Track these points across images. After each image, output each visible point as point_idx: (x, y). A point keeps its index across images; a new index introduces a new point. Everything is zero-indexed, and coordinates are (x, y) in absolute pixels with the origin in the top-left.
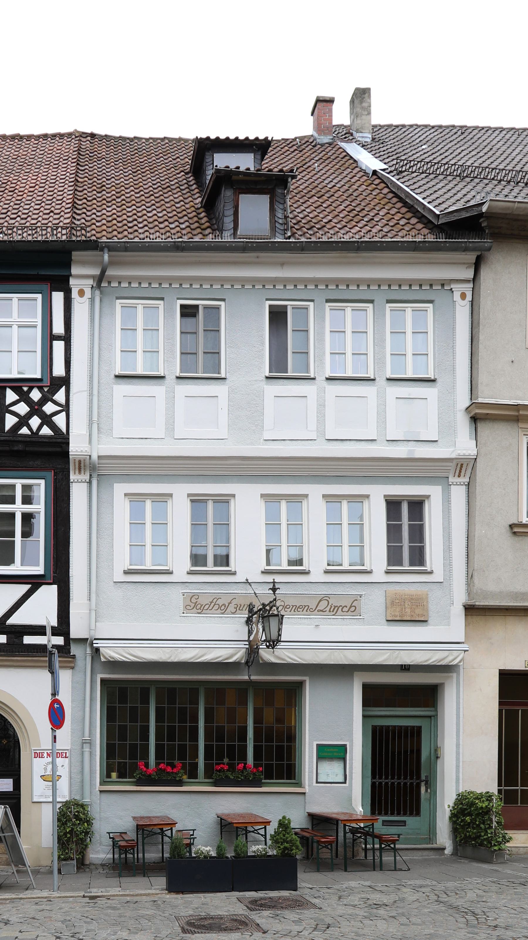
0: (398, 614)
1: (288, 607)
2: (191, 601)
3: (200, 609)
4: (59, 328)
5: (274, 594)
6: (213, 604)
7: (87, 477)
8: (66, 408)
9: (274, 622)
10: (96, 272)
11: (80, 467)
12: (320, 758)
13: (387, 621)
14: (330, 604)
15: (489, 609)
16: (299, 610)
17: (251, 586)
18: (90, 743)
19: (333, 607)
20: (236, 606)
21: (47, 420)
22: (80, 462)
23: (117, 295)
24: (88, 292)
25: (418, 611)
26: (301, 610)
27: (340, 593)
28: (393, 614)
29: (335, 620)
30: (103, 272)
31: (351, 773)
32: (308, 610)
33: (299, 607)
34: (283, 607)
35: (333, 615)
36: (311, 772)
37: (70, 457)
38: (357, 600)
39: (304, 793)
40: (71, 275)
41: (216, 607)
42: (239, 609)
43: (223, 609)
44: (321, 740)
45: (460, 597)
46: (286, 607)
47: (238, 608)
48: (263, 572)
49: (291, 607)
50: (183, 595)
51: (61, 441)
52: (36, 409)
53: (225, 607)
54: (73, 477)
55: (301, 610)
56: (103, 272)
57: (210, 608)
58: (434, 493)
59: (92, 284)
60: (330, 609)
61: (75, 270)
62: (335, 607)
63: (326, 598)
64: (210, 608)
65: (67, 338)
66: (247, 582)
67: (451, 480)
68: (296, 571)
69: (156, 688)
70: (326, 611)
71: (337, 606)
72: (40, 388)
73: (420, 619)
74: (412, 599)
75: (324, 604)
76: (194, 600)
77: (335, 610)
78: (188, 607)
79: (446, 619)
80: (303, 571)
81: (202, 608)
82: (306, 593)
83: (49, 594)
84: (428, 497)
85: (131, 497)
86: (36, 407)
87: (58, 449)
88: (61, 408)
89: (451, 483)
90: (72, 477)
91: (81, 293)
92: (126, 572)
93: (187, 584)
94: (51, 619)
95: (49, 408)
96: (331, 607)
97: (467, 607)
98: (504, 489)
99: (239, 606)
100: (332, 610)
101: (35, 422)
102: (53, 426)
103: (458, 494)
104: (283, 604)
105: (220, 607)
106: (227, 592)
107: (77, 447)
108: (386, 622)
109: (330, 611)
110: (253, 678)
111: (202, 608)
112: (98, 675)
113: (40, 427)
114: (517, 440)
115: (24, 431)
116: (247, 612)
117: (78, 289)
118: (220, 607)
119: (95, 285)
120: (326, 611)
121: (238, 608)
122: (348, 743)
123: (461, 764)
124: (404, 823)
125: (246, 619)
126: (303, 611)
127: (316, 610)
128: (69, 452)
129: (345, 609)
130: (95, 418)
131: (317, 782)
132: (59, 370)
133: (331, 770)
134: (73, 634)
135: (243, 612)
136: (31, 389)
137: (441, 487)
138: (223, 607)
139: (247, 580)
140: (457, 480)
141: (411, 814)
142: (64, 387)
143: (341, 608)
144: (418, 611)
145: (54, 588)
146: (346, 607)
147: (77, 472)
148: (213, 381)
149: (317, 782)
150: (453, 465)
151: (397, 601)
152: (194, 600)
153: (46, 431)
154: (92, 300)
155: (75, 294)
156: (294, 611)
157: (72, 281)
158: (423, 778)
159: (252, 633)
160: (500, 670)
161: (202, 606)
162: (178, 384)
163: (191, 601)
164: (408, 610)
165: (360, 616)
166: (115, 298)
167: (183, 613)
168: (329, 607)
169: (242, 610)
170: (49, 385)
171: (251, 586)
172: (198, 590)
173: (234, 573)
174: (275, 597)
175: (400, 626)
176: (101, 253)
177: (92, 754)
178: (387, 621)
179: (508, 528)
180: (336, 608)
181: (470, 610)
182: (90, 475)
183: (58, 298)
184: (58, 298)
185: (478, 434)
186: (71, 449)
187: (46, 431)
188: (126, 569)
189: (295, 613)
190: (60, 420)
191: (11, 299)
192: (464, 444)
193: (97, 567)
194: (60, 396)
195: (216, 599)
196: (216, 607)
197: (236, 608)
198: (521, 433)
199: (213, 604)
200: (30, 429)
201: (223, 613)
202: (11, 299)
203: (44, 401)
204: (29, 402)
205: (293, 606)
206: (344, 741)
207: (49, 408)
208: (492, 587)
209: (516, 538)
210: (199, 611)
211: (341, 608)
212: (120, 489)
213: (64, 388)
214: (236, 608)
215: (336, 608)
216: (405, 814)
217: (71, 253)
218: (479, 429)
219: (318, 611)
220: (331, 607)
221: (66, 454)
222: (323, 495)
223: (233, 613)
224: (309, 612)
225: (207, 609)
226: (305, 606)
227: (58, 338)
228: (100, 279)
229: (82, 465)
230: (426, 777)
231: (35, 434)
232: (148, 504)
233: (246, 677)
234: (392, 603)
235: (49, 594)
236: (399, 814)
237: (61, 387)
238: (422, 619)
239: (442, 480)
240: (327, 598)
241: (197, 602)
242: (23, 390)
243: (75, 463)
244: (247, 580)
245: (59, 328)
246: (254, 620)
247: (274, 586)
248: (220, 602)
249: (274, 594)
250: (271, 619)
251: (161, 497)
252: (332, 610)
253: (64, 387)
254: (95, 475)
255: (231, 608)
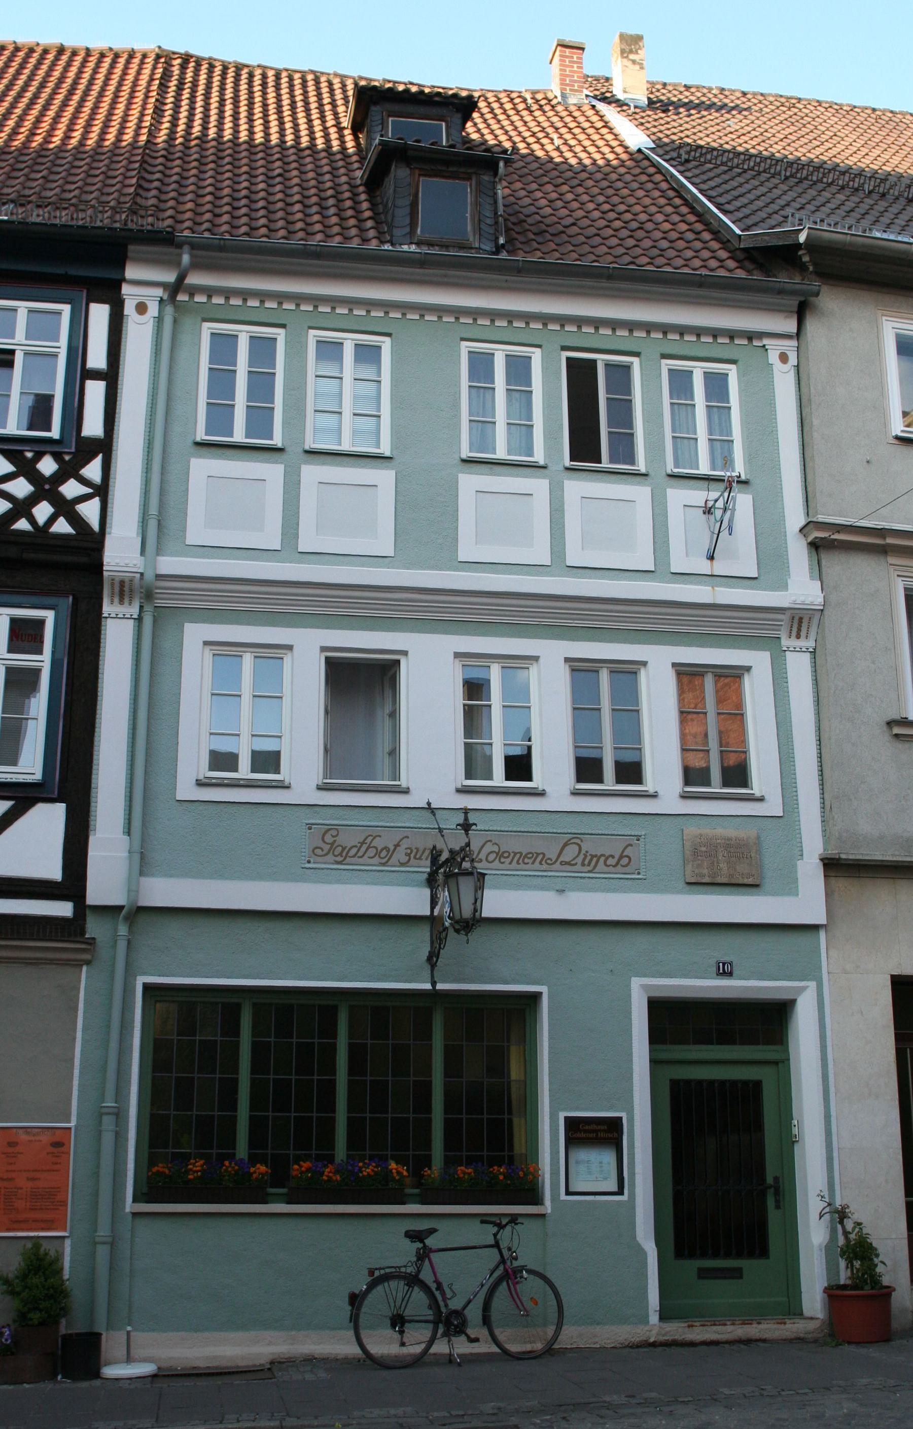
0: (706, 871)
1: (506, 855)
2: (323, 839)
3: (341, 854)
4: (97, 358)
5: (467, 834)
6: (365, 847)
7: (134, 610)
8: (102, 491)
9: (466, 886)
10: (170, 277)
11: (124, 590)
12: (571, 1142)
13: (689, 884)
14: (583, 852)
15: (865, 866)
16: (526, 860)
17: (434, 815)
18: (119, 1115)
19: (589, 858)
20: (409, 851)
21: (65, 508)
22: (122, 583)
23: (205, 316)
24: (153, 309)
25: (742, 868)
26: (530, 861)
27: (600, 832)
28: (696, 871)
29: (593, 881)
30: (181, 278)
31: (632, 1174)
32: (543, 862)
33: (526, 856)
34: (497, 854)
35: (589, 872)
36: (555, 1173)
37: (105, 573)
38: (631, 845)
39: (543, 1216)
40: (124, 280)
41: (372, 852)
42: (415, 858)
43: (385, 855)
44: (571, 1110)
45: (813, 846)
46: (502, 856)
47: (412, 856)
48: (458, 791)
49: (512, 854)
50: (310, 829)
51: (89, 544)
52: (46, 489)
53: (388, 851)
54: (107, 608)
55: (530, 861)
56: (181, 278)
57: (360, 854)
58: (758, 661)
59: (161, 295)
60: (584, 860)
61: (132, 272)
62: (593, 856)
63: (574, 839)
64: (360, 854)
65: (111, 376)
66: (430, 808)
67: (785, 642)
68: (513, 790)
69: (254, 1005)
70: (576, 864)
71: (596, 856)
72: (57, 457)
73: (746, 881)
74: (729, 846)
75: (570, 853)
76: (329, 838)
77: (592, 861)
78: (318, 851)
79: (789, 886)
80: (533, 791)
81: (344, 854)
82: (539, 830)
83: (48, 821)
84: (748, 669)
85: (214, 648)
86: (47, 487)
87: (84, 560)
88: (91, 491)
89: (785, 649)
90: (107, 609)
91: (141, 308)
92: (200, 784)
93: (317, 809)
94: (52, 869)
95: (71, 489)
96: (586, 856)
97: (826, 861)
98: (873, 663)
99: (415, 851)
100: (586, 862)
101: (43, 511)
102: (76, 520)
103: (799, 667)
104: (496, 849)
105: (378, 853)
106: (392, 824)
107: (121, 554)
108: (685, 885)
109: (583, 865)
110: (439, 986)
111: (344, 854)
112: (138, 978)
113: (52, 520)
114: (892, 583)
115: (22, 525)
116: (428, 863)
117: (136, 302)
118: (378, 853)
119: (165, 297)
120: (576, 864)
121: (413, 854)
122: (624, 1115)
123: (835, 1154)
124: (736, 1274)
125: (425, 876)
126: (533, 863)
127: (558, 862)
128: (102, 565)
129: (611, 861)
130: (153, 510)
131: (568, 1193)
132: (93, 426)
133: (594, 1168)
134: (92, 898)
135: (423, 863)
136: (39, 456)
137: (767, 654)
138: (384, 854)
139: (429, 804)
140: (794, 643)
141: (751, 1255)
142: (100, 456)
143: (602, 859)
144: (742, 868)
145: (58, 811)
146: (613, 857)
147: (116, 600)
148: (368, 460)
149: (568, 1193)
150: (785, 617)
151: (704, 849)
152: (329, 838)
153: (62, 526)
154: (159, 320)
155: (129, 308)
156: (518, 863)
157: (126, 289)
158: (770, 1180)
159: (436, 904)
160: (892, 977)
161: (344, 849)
162: (306, 463)
163: (323, 839)
164: (723, 866)
165: (639, 873)
166: (200, 319)
167: (309, 862)
168: (582, 856)
169: (420, 859)
170: (73, 450)
171: (434, 815)
172: (338, 819)
173: (406, 791)
174: (467, 840)
175: (712, 893)
176: (178, 251)
177: (120, 1136)
178: (689, 884)
179: (885, 728)
180: (595, 859)
181: (833, 866)
182: (141, 607)
183: (99, 314)
184: (99, 314)
185: (824, 570)
186: (106, 560)
187: (62, 526)
188: (201, 777)
189: (519, 867)
190: (90, 511)
191: (15, 310)
192: (802, 588)
193: (146, 773)
194: (93, 470)
195: (371, 838)
196: (372, 852)
197: (409, 855)
198: (893, 574)
199: (365, 847)
200: (32, 520)
201: (384, 864)
202: (15, 310)
203: (60, 477)
204: (34, 477)
205: (515, 854)
206: (616, 1111)
207: (71, 489)
208: (865, 827)
209: (900, 745)
210: (339, 859)
211: (602, 859)
212: (195, 634)
213: (99, 458)
214: (409, 855)
215: (595, 859)
216: (739, 1255)
217: (127, 247)
218: (824, 563)
219: (561, 863)
220: (586, 856)
221: (97, 567)
222: (565, 658)
223: (402, 864)
224: (545, 867)
225: (354, 856)
226: (538, 854)
227: (96, 375)
228: (175, 289)
229: (126, 589)
230: (776, 1179)
231: (42, 531)
232: (248, 659)
233: (428, 986)
234: (696, 853)
235: (48, 821)
236: (728, 1255)
237: (94, 456)
238: (750, 881)
239: (771, 643)
240: (579, 842)
241: (335, 841)
242: (25, 457)
243: (113, 584)
244: (429, 804)
245: (97, 358)
246: (440, 877)
247: (466, 819)
248: (379, 843)
249: (467, 834)
250: (462, 880)
251: (276, 651)
252: (586, 862)
253: (100, 456)
254: (148, 608)
255: (400, 855)
